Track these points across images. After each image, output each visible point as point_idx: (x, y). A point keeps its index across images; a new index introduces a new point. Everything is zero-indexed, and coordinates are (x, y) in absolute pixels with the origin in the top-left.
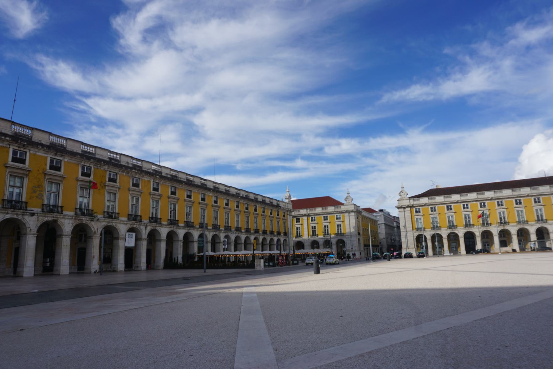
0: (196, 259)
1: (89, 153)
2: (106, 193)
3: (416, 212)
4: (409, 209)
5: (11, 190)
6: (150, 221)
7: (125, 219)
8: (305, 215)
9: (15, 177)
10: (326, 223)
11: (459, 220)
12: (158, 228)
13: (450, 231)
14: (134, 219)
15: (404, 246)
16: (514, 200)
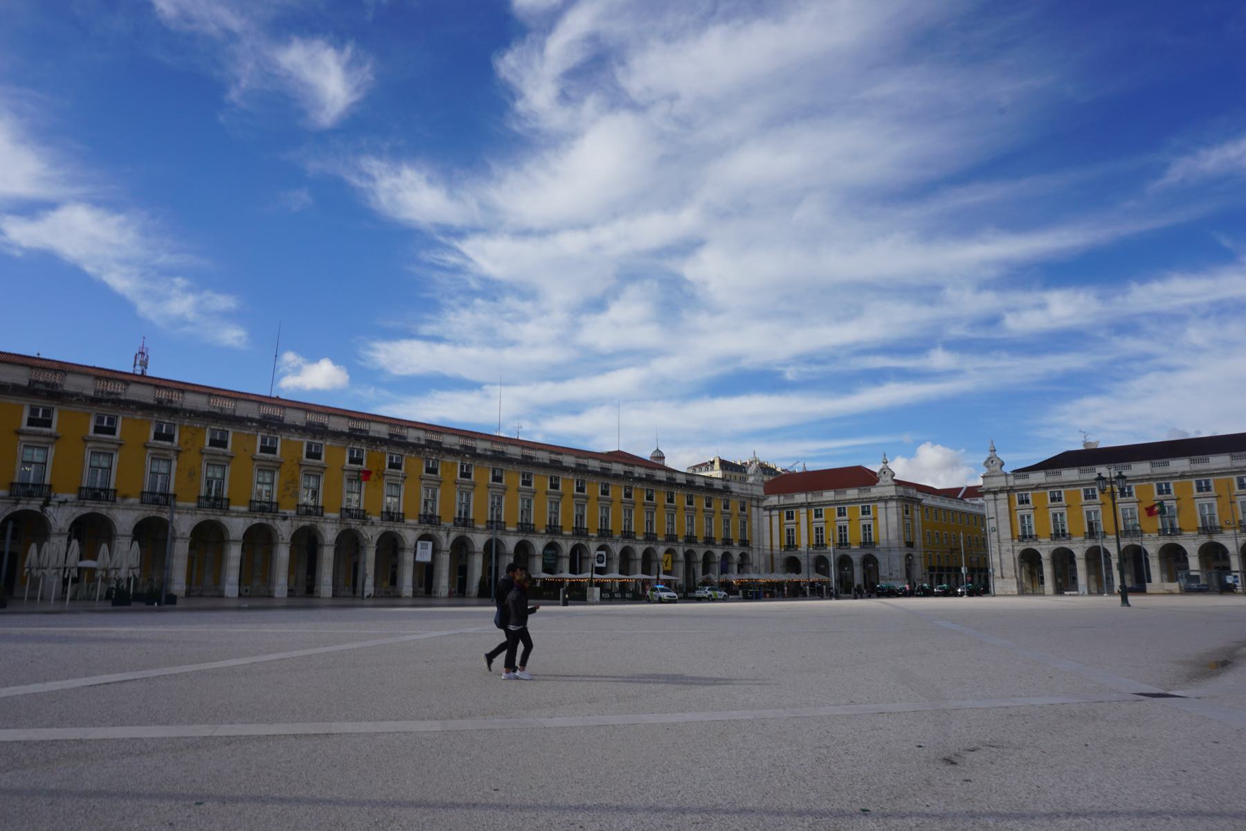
0: (538, 585)
1: (361, 430)
3: (1021, 502)
4: (1005, 495)
5: (259, 487)
6: (455, 524)
7: (415, 521)
9: (264, 471)
10: (843, 521)
12: (469, 535)
13: (1089, 543)
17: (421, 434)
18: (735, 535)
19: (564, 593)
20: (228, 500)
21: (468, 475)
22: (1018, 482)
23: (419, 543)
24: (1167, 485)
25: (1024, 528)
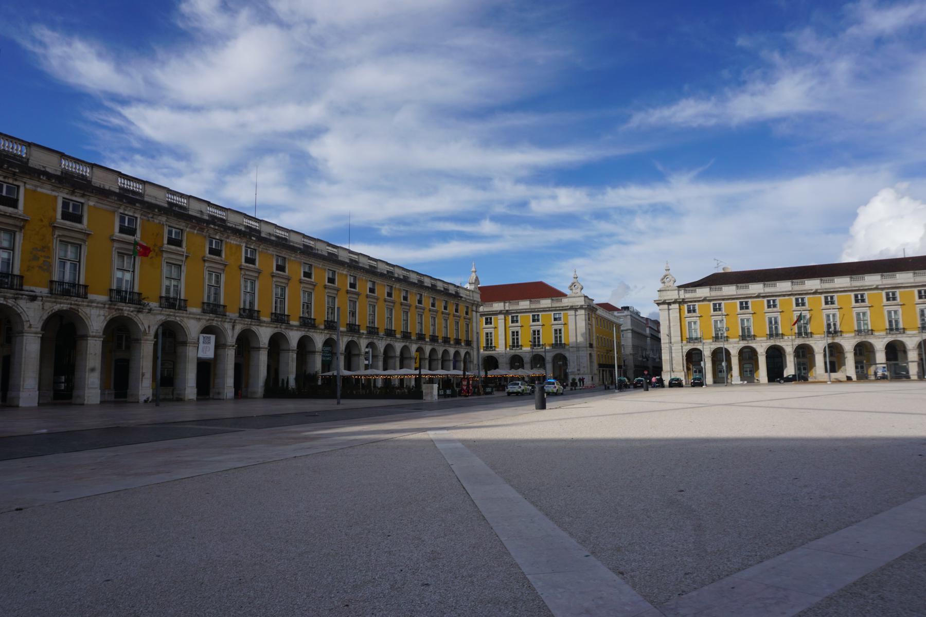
0: (320, 383)
1: (133, 192)
3: (689, 311)
4: (677, 306)
6: (240, 316)
8: (500, 312)
10: (536, 326)
11: (759, 327)
12: (254, 328)
13: (743, 344)
14: (214, 312)
15: (666, 367)
16: (852, 294)
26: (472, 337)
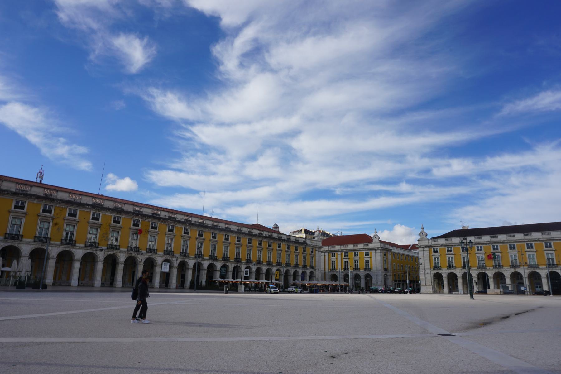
1: (139, 211)
2: (149, 237)
3: (435, 252)
4: (427, 249)
5: (90, 236)
9: (93, 228)
12: (186, 260)
14: (168, 254)
17: (167, 214)
18: (308, 263)
19: (226, 287)
20: (75, 241)
21: (188, 233)
22: (433, 243)
23: (163, 263)
24: (497, 246)
25: (435, 263)
26: (315, 264)
